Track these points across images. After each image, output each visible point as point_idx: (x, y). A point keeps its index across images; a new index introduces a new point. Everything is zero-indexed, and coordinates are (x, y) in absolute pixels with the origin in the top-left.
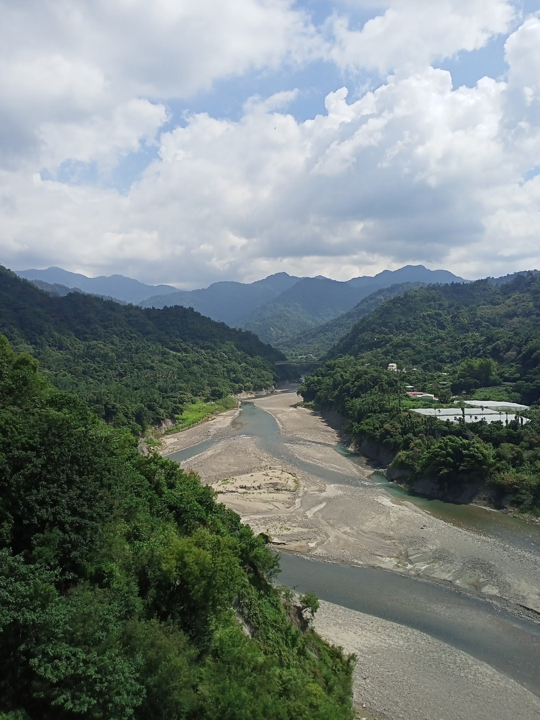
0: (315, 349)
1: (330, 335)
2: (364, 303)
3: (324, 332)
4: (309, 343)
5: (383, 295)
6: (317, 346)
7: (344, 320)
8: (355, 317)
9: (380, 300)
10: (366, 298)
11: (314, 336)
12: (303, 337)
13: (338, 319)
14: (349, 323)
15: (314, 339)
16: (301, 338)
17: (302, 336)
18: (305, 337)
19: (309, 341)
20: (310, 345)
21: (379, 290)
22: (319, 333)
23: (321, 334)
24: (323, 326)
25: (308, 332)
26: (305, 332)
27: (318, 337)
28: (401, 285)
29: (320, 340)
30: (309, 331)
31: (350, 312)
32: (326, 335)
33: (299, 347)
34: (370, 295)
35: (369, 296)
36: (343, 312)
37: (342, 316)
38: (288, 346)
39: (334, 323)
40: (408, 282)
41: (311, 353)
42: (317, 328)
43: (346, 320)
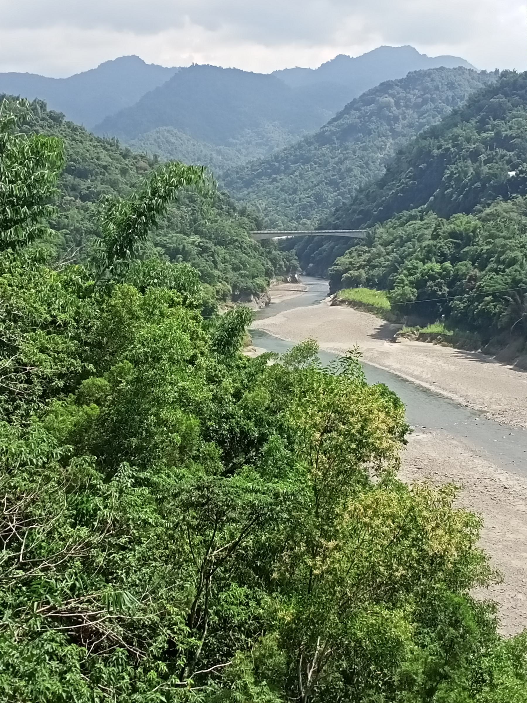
2: (353, 112)
3: (270, 175)
5: (393, 95)
7: (312, 147)
8: (336, 141)
9: (388, 106)
10: (355, 101)
11: (248, 184)
12: (225, 185)
13: (300, 146)
14: (324, 155)
15: (250, 190)
19: (240, 195)
21: (382, 84)
22: (259, 176)
23: (265, 180)
24: (268, 162)
25: (235, 176)
26: (226, 175)
28: (428, 74)
30: (237, 173)
31: (324, 132)
32: (275, 180)
34: (364, 94)
35: (361, 97)
36: (312, 131)
40: (442, 68)
43: (316, 148)
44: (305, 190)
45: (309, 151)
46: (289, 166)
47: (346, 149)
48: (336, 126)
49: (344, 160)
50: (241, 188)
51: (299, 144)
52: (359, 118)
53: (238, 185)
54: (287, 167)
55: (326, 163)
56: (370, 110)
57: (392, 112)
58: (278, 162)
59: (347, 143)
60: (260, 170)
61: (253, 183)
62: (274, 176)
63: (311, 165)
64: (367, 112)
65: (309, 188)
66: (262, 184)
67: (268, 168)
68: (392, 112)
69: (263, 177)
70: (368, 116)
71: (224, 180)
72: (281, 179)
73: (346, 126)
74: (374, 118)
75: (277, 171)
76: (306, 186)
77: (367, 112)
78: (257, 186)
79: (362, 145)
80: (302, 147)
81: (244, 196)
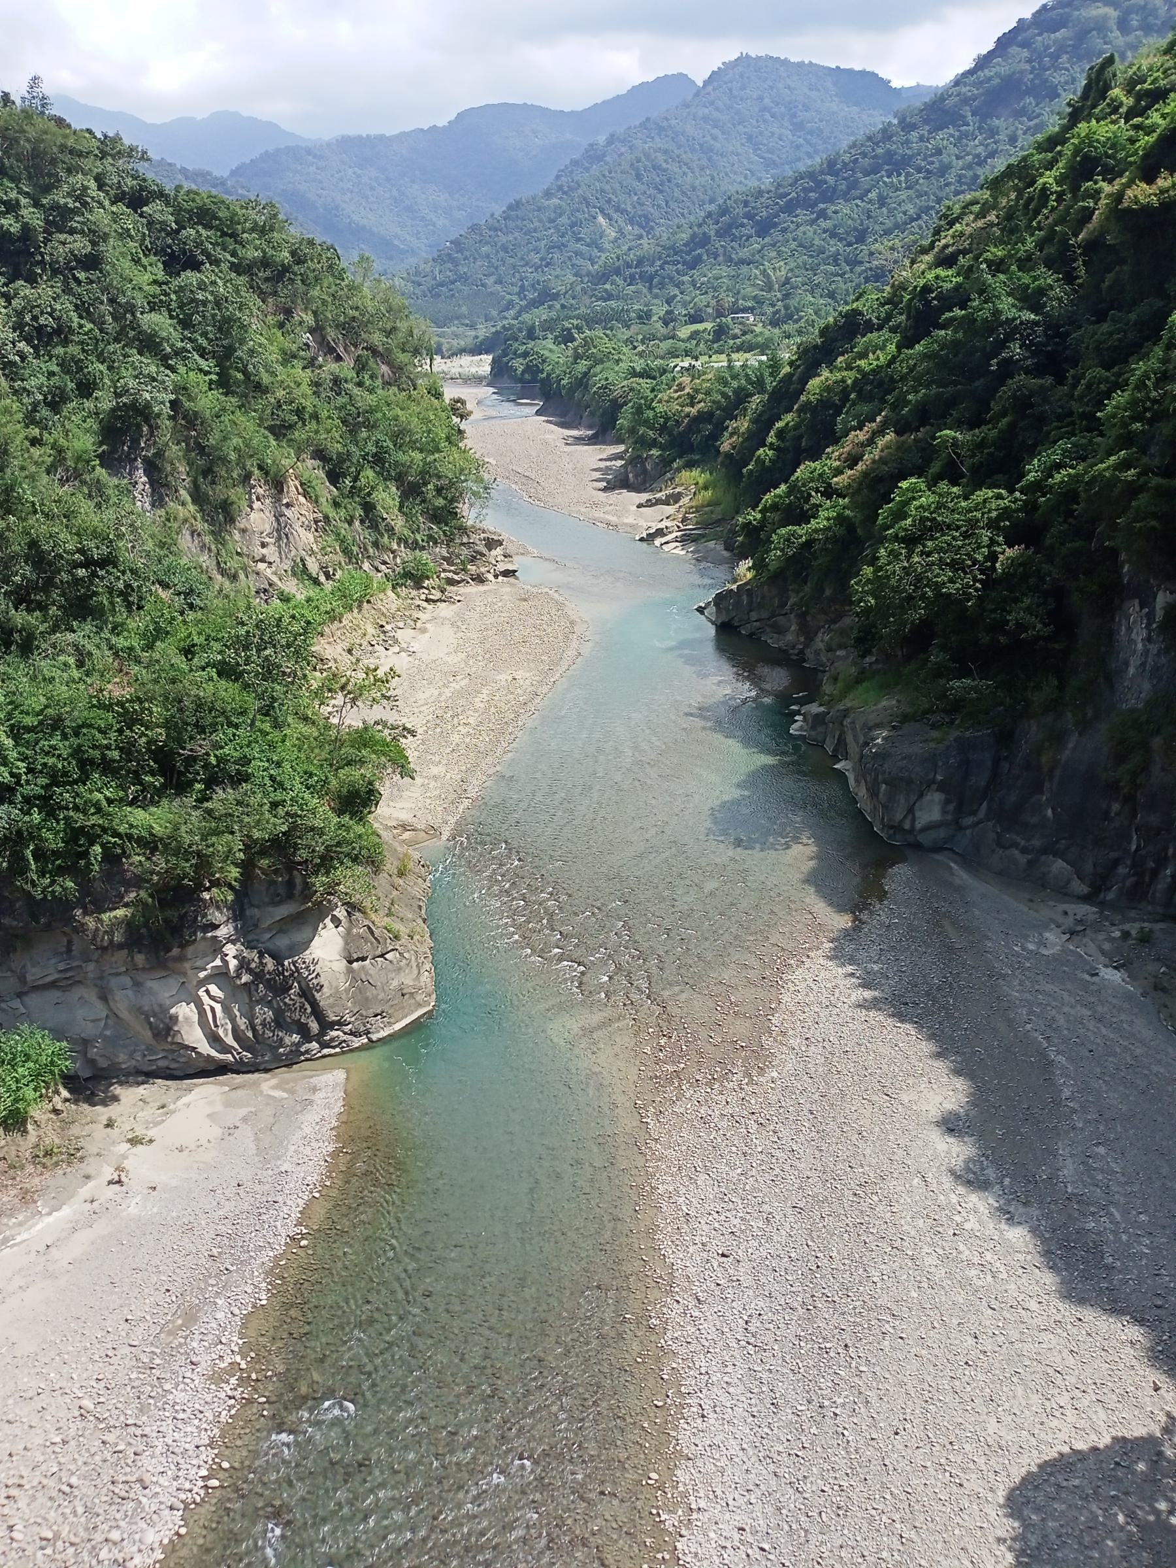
0: (769, 287)
1: (845, 211)
4: (743, 262)
6: (779, 271)
7: (914, 135)
9: (1100, 27)
11: (764, 229)
12: (717, 232)
14: (939, 152)
15: (767, 240)
16: (705, 241)
17: (711, 230)
18: (720, 234)
19: (744, 253)
20: (744, 269)
22: (790, 208)
23: (803, 215)
24: (811, 175)
25: (740, 210)
26: (724, 211)
27: (784, 230)
29: (793, 245)
30: (746, 204)
32: (823, 214)
33: (693, 284)
37: (902, 121)
38: (648, 279)
39: (864, 155)
41: (751, 310)
42: (779, 186)
43: (921, 139)
44: (887, 232)
45: (908, 142)
46: (856, 181)
47: (993, 132)
48: (974, 84)
49: (986, 157)
50: (749, 237)
51: (884, 131)
52: (1030, 61)
53: (745, 231)
54: (854, 185)
55: (944, 169)
56: (1055, 41)
57: (1110, 43)
58: (835, 174)
59: (996, 122)
60: (794, 194)
61: (775, 225)
62: (822, 206)
63: (908, 175)
64: (1048, 47)
65: (897, 226)
66: (792, 226)
67: (811, 190)
68: (1110, 43)
69: (798, 211)
70: (1051, 56)
71: (717, 223)
72: (836, 212)
73: (997, 81)
74: (1065, 57)
75: (829, 196)
76: (889, 223)
77: (1048, 47)
78: (784, 230)
79: (1032, 123)
80: (891, 137)
81: (753, 255)
